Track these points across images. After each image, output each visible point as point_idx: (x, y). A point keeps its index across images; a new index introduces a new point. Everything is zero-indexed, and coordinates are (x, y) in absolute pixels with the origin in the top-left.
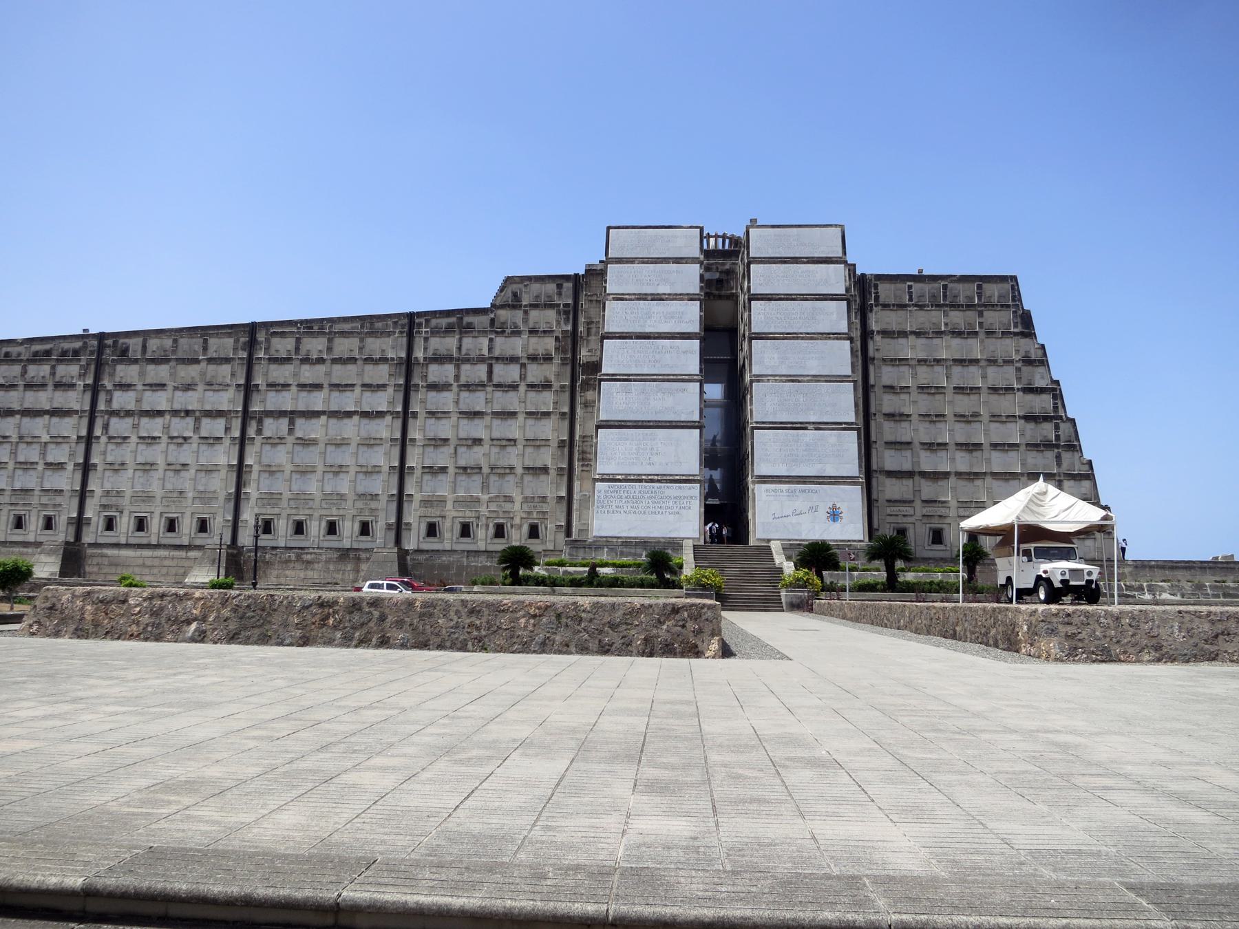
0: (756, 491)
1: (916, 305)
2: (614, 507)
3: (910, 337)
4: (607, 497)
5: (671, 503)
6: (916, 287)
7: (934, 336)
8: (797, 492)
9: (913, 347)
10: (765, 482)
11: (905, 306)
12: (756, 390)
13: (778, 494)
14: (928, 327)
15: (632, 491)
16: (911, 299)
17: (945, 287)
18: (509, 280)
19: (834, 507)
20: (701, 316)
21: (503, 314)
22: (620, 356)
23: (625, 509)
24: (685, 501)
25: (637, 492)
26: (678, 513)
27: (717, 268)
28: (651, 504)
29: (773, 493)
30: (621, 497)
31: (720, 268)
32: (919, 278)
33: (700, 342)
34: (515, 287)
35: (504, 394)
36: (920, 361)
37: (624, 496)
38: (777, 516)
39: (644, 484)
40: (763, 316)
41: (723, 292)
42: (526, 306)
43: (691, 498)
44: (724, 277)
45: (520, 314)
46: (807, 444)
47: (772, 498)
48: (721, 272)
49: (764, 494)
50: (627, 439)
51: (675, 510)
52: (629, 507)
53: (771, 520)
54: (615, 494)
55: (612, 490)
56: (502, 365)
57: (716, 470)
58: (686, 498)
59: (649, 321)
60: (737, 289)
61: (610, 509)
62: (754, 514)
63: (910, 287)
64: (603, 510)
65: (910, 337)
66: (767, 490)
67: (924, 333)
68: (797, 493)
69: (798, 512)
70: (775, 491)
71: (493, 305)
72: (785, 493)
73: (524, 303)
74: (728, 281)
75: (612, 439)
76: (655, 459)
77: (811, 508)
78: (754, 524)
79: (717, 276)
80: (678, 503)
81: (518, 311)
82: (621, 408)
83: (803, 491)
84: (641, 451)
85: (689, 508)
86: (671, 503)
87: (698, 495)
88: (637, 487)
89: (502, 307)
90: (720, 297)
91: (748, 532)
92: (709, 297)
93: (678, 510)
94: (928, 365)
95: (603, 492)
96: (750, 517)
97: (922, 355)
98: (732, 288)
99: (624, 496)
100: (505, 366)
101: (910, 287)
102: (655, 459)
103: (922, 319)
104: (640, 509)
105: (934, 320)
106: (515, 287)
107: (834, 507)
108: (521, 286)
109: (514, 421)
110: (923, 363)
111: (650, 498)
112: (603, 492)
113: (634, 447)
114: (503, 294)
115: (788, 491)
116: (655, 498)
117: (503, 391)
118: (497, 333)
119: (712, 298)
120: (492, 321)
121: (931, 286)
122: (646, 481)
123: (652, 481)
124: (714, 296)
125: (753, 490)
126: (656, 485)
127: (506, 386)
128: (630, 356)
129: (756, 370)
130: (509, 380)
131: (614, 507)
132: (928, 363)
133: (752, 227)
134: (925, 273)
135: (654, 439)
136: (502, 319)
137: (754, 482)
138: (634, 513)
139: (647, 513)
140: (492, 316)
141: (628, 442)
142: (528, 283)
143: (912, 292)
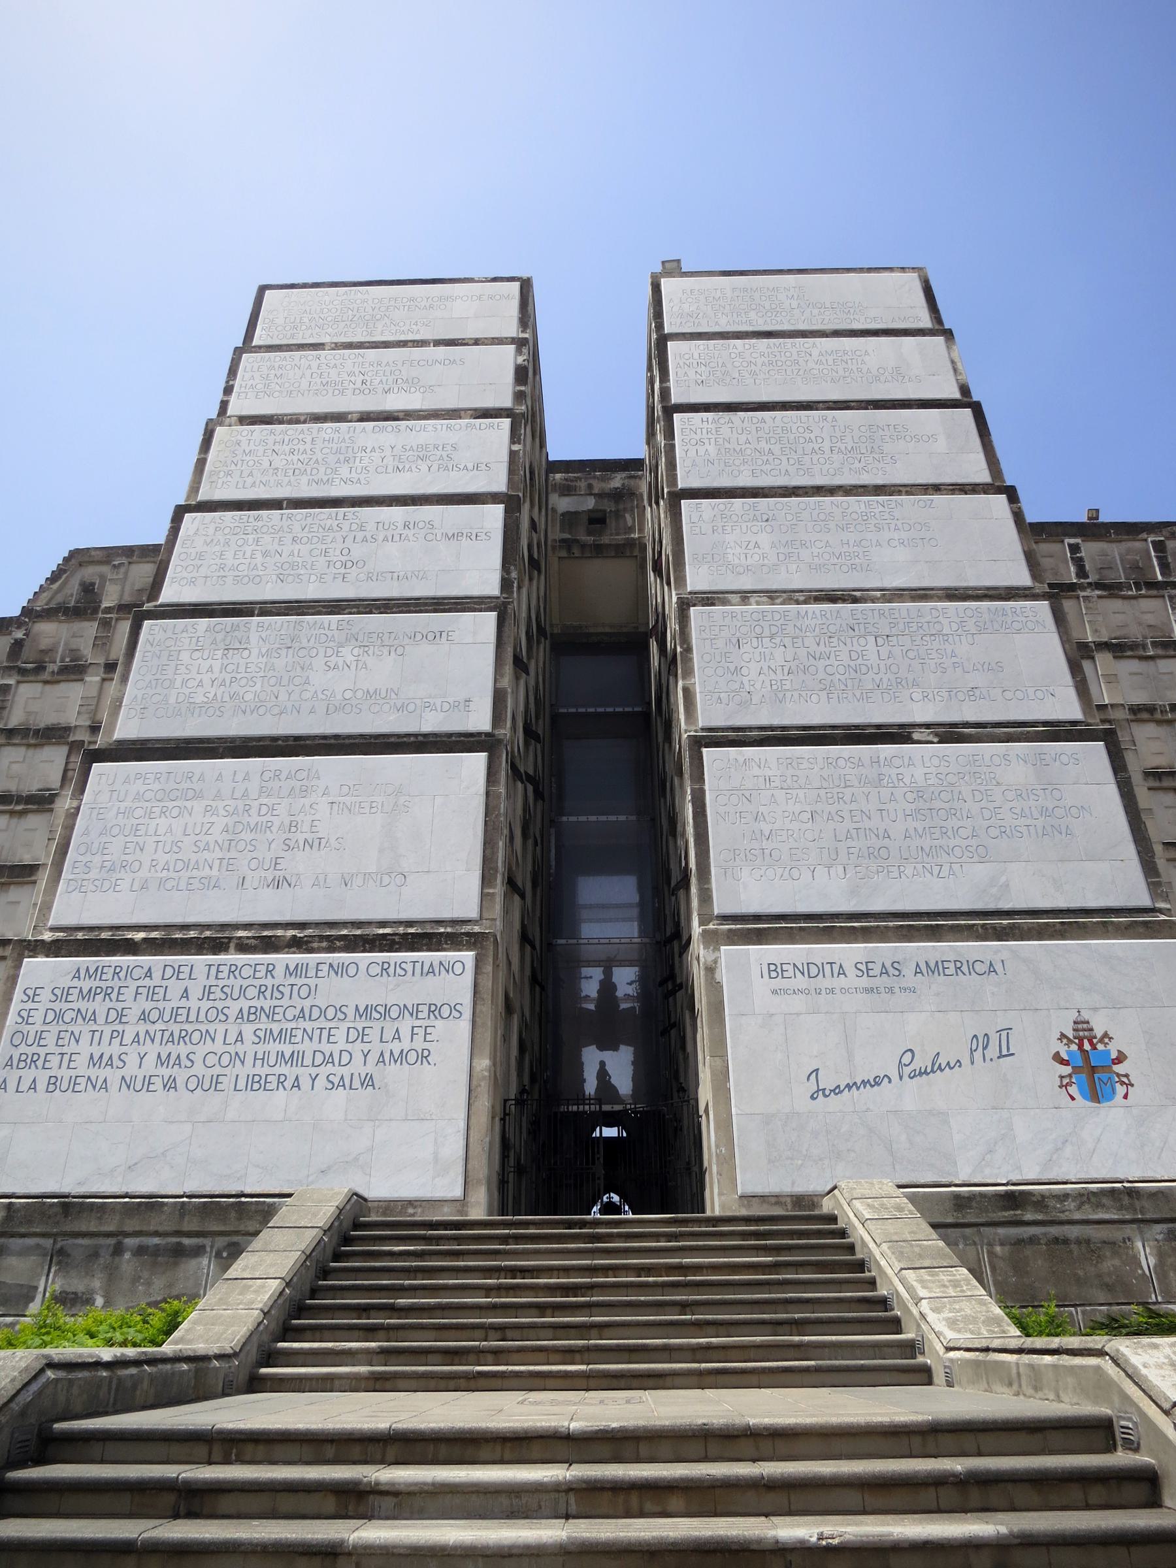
0: (724, 975)
1: (1097, 586)
2: (81, 1061)
3: (1099, 657)
4: (59, 1016)
5: (340, 1035)
6: (1090, 550)
7: (1160, 652)
8: (909, 971)
9: (1112, 679)
10: (759, 937)
11: (1072, 587)
12: (702, 630)
13: (825, 983)
14: (1135, 633)
15: (176, 988)
16: (1082, 572)
17: (1159, 547)
18: (78, 558)
19: (1083, 1034)
20: (513, 455)
21: (48, 632)
22: (229, 555)
23: (131, 1069)
24: (406, 1024)
25: (196, 992)
26: (368, 1081)
27: (590, 486)
28: (248, 1047)
29: (801, 982)
30: (121, 1015)
31: (598, 487)
32: (1093, 529)
33: (506, 511)
34: (90, 573)
35: (14, 821)
36: (1135, 710)
37: (133, 1015)
38: (827, 1083)
39: (233, 958)
40: (712, 449)
41: (605, 540)
42: (108, 610)
43: (434, 1010)
44: (608, 506)
45: (90, 629)
46: (919, 793)
47: (797, 1003)
48: (600, 496)
49: (761, 986)
50: (199, 796)
51: (358, 1067)
52: (151, 1059)
53: (802, 1103)
54: (99, 1006)
55: (86, 985)
56: (23, 750)
57: (615, 1048)
58: (414, 1012)
59: (344, 471)
60: (641, 530)
61: (65, 1073)
62: (722, 1078)
63: (1075, 548)
64: (28, 1075)
65: (1099, 657)
66: (775, 970)
67: (1134, 646)
68: (909, 979)
69: (918, 1064)
70: (804, 970)
71: (26, 611)
72: (852, 979)
73: (105, 605)
74: (618, 515)
75: (138, 797)
76: (299, 863)
77: (980, 1042)
78: (726, 1125)
79: (590, 503)
80: (373, 1034)
81: (86, 624)
82: (199, 699)
83: (936, 968)
84: (247, 836)
85: (424, 1057)
86: (340, 1035)
87: (466, 999)
88: (200, 972)
89: (49, 614)
90: (599, 550)
91: (702, 1173)
92: (569, 550)
93: (370, 1068)
94: (1159, 722)
95: (45, 996)
96: (705, 1094)
97: (1139, 698)
98: (631, 529)
99: (133, 1015)
100: (31, 752)
101: (1075, 548)
102: (299, 863)
103: (1120, 617)
104: (198, 1069)
105: (1150, 619)
106: (90, 573)
107: (1083, 1034)
108: (105, 569)
109: (26, 889)
110: (1145, 716)
111: (253, 1015)
112: (45, 996)
113: (220, 822)
114: (55, 586)
115: (865, 968)
116: (271, 1015)
117: (12, 813)
118: (22, 672)
119: (576, 552)
120: (18, 645)
121: (1125, 546)
122: (243, 947)
123: (269, 945)
124: (583, 546)
125: (711, 970)
126: (281, 959)
127: (20, 799)
128: (265, 554)
129: (697, 579)
130: (32, 786)
131: (81, 1061)
132: (1158, 716)
133: (668, 273)
134: (1104, 518)
135: (305, 791)
136: (44, 643)
137: (713, 940)
138: (170, 1085)
139: (226, 1083)
140: (19, 634)
141: (198, 806)
142: (124, 560)
143: (1081, 559)
